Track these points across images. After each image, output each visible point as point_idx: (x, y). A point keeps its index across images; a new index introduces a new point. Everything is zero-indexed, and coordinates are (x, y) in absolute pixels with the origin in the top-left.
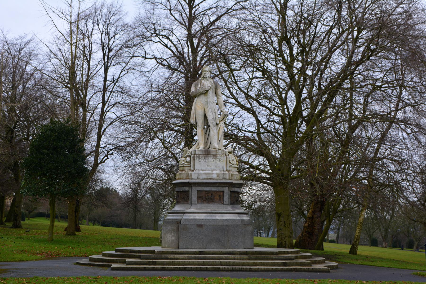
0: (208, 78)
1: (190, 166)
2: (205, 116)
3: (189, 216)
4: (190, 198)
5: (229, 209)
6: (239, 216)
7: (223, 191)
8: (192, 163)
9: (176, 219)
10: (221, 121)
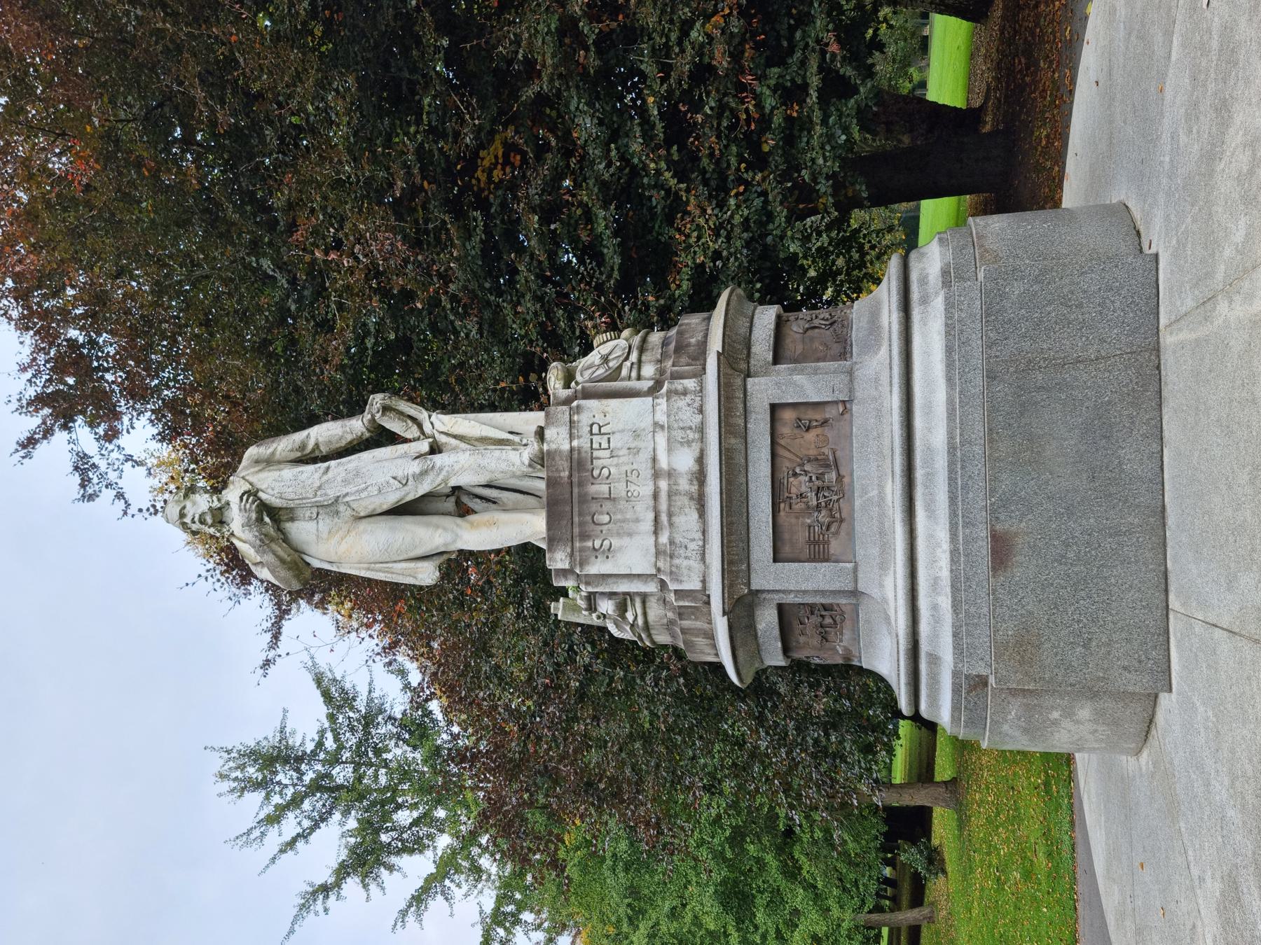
0: (216, 504)
1: (644, 597)
2: (402, 510)
4: (819, 600)
5: (877, 365)
7: (774, 408)
8: (623, 587)
9: (956, 690)
10: (420, 426)
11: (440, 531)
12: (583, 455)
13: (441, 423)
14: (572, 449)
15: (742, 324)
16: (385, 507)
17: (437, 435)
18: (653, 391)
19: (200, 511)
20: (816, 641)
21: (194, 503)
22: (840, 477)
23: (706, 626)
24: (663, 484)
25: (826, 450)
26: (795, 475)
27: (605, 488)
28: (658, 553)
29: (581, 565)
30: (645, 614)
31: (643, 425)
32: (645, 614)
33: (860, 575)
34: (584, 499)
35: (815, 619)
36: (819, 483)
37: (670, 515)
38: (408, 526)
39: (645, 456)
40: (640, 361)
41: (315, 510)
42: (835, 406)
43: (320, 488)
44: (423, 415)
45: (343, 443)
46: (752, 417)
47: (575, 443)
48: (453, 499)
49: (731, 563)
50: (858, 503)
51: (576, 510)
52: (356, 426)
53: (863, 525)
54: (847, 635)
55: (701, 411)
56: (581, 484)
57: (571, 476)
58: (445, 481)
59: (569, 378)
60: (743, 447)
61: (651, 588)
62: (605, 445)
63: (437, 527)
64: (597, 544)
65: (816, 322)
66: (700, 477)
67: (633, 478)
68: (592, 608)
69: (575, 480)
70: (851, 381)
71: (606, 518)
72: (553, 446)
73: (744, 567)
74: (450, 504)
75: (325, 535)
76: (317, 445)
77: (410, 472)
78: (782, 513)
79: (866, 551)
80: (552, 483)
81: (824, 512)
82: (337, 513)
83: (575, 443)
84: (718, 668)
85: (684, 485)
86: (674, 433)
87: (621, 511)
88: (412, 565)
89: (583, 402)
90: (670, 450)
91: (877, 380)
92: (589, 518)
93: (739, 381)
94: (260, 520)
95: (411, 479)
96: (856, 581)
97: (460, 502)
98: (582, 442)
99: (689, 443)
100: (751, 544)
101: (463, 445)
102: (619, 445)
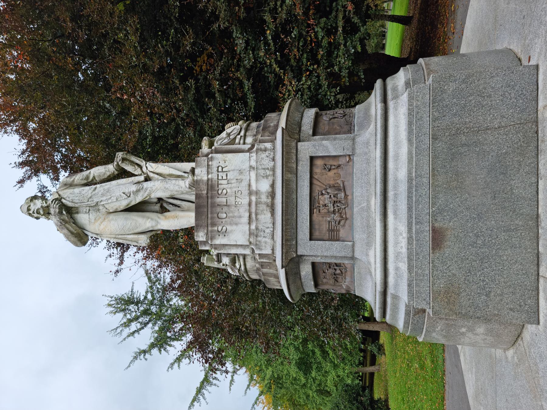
1: (244, 256)
3: (398, 276)
4: (333, 261)
5: (368, 136)
6: (396, 97)
7: (312, 159)
8: (233, 251)
10: (141, 167)
11: (149, 220)
12: (214, 182)
13: (152, 167)
14: (208, 180)
15: (297, 116)
16: (122, 208)
17: (149, 173)
18: (249, 150)
19: (37, 208)
20: (332, 281)
21: (35, 204)
22: (346, 196)
23: (275, 272)
24: (254, 198)
25: (339, 182)
26: (322, 194)
27: (224, 200)
28: (250, 234)
29: (212, 239)
30: (245, 265)
31: (244, 167)
32: (245, 265)
33: (356, 249)
34: (214, 205)
35: (331, 271)
36: (335, 199)
37: (256, 214)
38: (134, 217)
39: (245, 183)
40: (245, 136)
41: (88, 208)
42: (344, 158)
43: (91, 197)
44: (143, 163)
45: (106, 176)
46: (300, 163)
47: (210, 176)
48: (159, 205)
49: (287, 240)
50: (355, 210)
51: (209, 210)
52: (110, 168)
53: (358, 222)
54: (348, 279)
55: (274, 160)
56: (212, 197)
57: (207, 193)
58: (149, 195)
59: (211, 145)
60: (295, 179)
61: (247, 252)
62: (225, 177)
63: (148, 218)
64: (220, 229)
65: (336, 115)
66: (272, 195)
67: (239, 195)
68: (219, 261)
69: (209, 195)
70: (354, 144)
71: (225, 215)
72: (199, 178)
73: (294, 242)
74: (157, 207)
75: (93, 221)
76: (94, 177)
77: (132, 190)
78: (315, 215)
79: (359, 236)
80: (198, 196)
81: (337, 215)
82: (99, 210)
83: (210, 176)
85: (264, 198)
86: (259, 171)
87: (232, 212)
88: (136, 236)
89: (214, 155)
90: (257, 180)
91: (368, 143)
92: (216, 215)
93: (294, 144)
94: (60, 213)
95: (132, 194)
96: (353, 252)
97: (162, 206)
98: (213, 176)
99: (267, 177)
100: (298, 230)
101: (161, 178)
102: (232, 178)
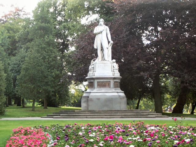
1: (94, 70)
5: (114, 91)
7: (110, 82)
79: (98, 89)
84: (87, 76)
